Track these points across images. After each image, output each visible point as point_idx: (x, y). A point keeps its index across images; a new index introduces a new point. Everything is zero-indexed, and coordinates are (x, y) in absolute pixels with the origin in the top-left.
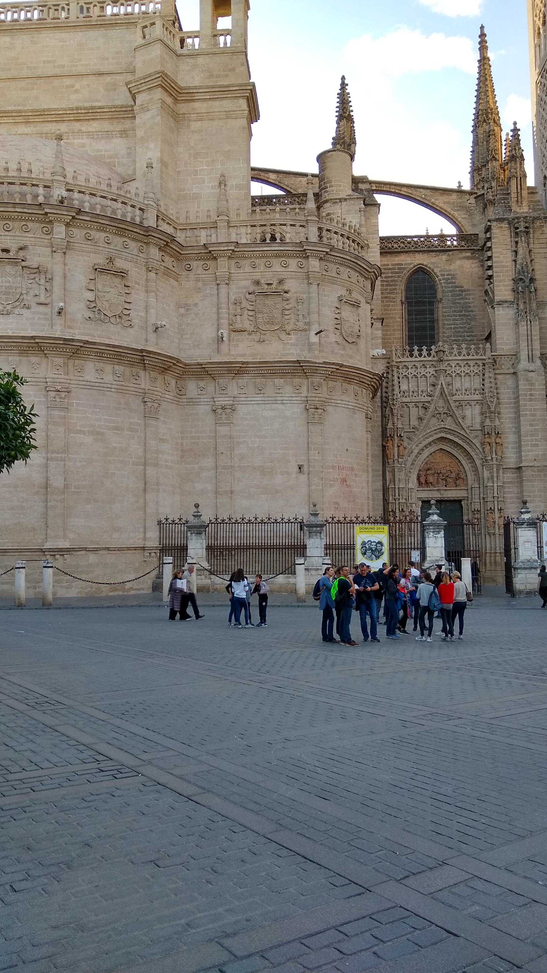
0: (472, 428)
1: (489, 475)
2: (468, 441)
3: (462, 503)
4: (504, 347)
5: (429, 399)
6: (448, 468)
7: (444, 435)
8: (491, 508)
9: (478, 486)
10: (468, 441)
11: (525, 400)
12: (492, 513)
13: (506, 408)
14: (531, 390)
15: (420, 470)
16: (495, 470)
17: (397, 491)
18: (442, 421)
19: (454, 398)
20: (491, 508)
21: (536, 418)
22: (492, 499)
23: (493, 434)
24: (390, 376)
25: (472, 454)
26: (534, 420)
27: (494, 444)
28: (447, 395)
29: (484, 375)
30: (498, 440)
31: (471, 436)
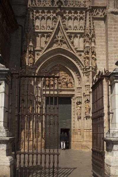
0: (78, 49)
5: (52, 31)
8: (88, 99)
11: (111, 31)
13: (99, 39)
16: (91, 75)
18: (59, 45)
19: (67, 31)
20: (88, 99)
22: (89, 94)
23: (90, 52)
24: (27, 15)
27: (91, 58)
29: (86, 18)
30: (93, 56)
31: (77, 55)
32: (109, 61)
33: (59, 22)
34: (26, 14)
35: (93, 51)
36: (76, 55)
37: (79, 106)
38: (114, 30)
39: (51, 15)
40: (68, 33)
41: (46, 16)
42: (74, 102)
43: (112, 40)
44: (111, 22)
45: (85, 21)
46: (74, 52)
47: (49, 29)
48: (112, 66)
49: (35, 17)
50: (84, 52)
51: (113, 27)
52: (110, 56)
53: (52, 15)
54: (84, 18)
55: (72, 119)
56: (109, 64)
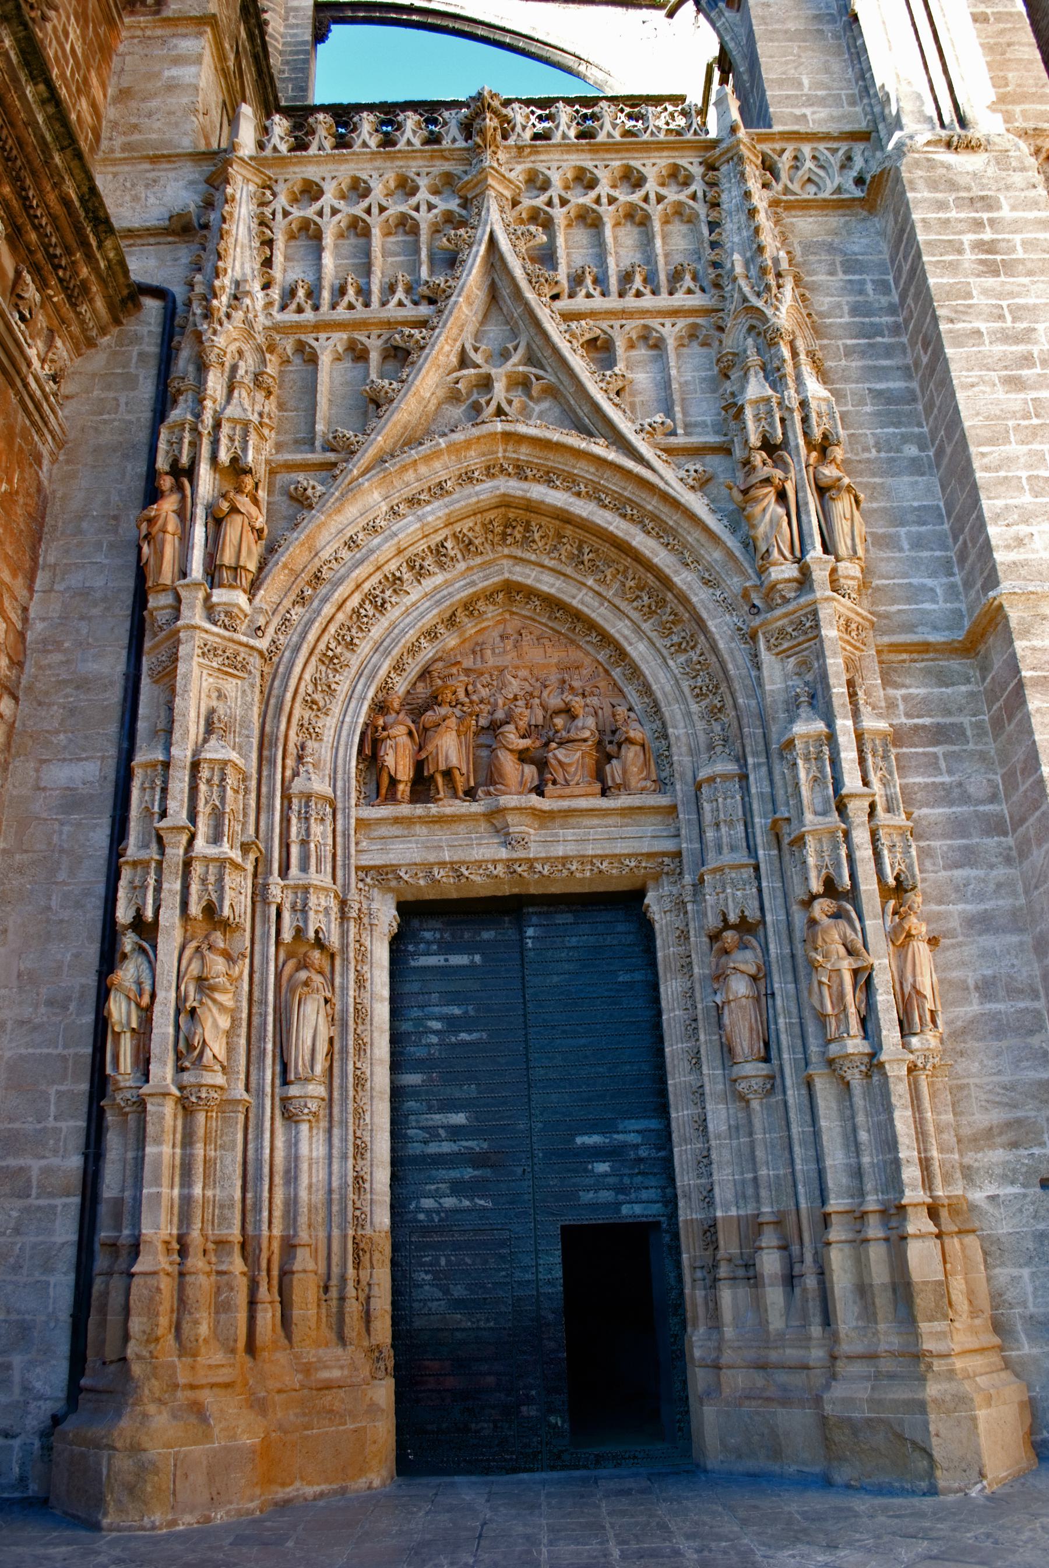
1: (796, 681)
2: (652, 504)
3: (650, 898)
4: (808, 111)
5: (424, 310)
6: (555, 702)
7: (512, 486)
9: (732, 767)
10: (652, 504)
11: (953, 267)
12: (837, 915)
14: (978, 225)
15: (380, 707)
17: (179, 784)
18: (500, 412)
19: (563, 304)
21: (1036, 350)
25: (683, 579)
26: (1027, 360)
28: (524, 284)
32: (985, 503)
33: (492, 241)
34: (209, 204)
35: (817, 434)
36: (662, 485)
37: (746, 960)
38: (982, 262)
39: (417, 209)
40: (568, 317)
41: (375, 210)
42: (684, 936)
43: (978, 333)
44: (942, 206)
45: (713, 225)
46: (640, 459)
47: (400, 304)
48: (1020, 542)
49: (280, 225)
50: (738, 453)
51: (968, 238)
52: (986, 460)
53: (431, 207)
54: (701, 208)
55: (681, 1114)
56: (992, 530)
